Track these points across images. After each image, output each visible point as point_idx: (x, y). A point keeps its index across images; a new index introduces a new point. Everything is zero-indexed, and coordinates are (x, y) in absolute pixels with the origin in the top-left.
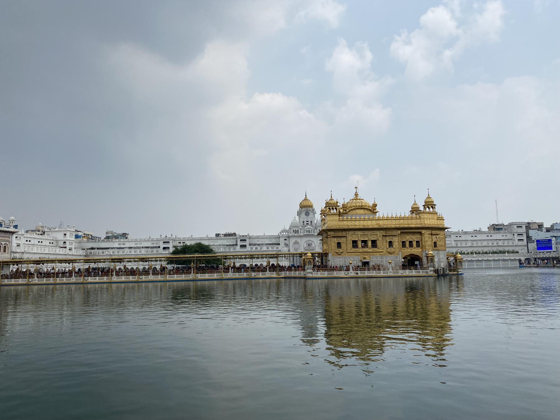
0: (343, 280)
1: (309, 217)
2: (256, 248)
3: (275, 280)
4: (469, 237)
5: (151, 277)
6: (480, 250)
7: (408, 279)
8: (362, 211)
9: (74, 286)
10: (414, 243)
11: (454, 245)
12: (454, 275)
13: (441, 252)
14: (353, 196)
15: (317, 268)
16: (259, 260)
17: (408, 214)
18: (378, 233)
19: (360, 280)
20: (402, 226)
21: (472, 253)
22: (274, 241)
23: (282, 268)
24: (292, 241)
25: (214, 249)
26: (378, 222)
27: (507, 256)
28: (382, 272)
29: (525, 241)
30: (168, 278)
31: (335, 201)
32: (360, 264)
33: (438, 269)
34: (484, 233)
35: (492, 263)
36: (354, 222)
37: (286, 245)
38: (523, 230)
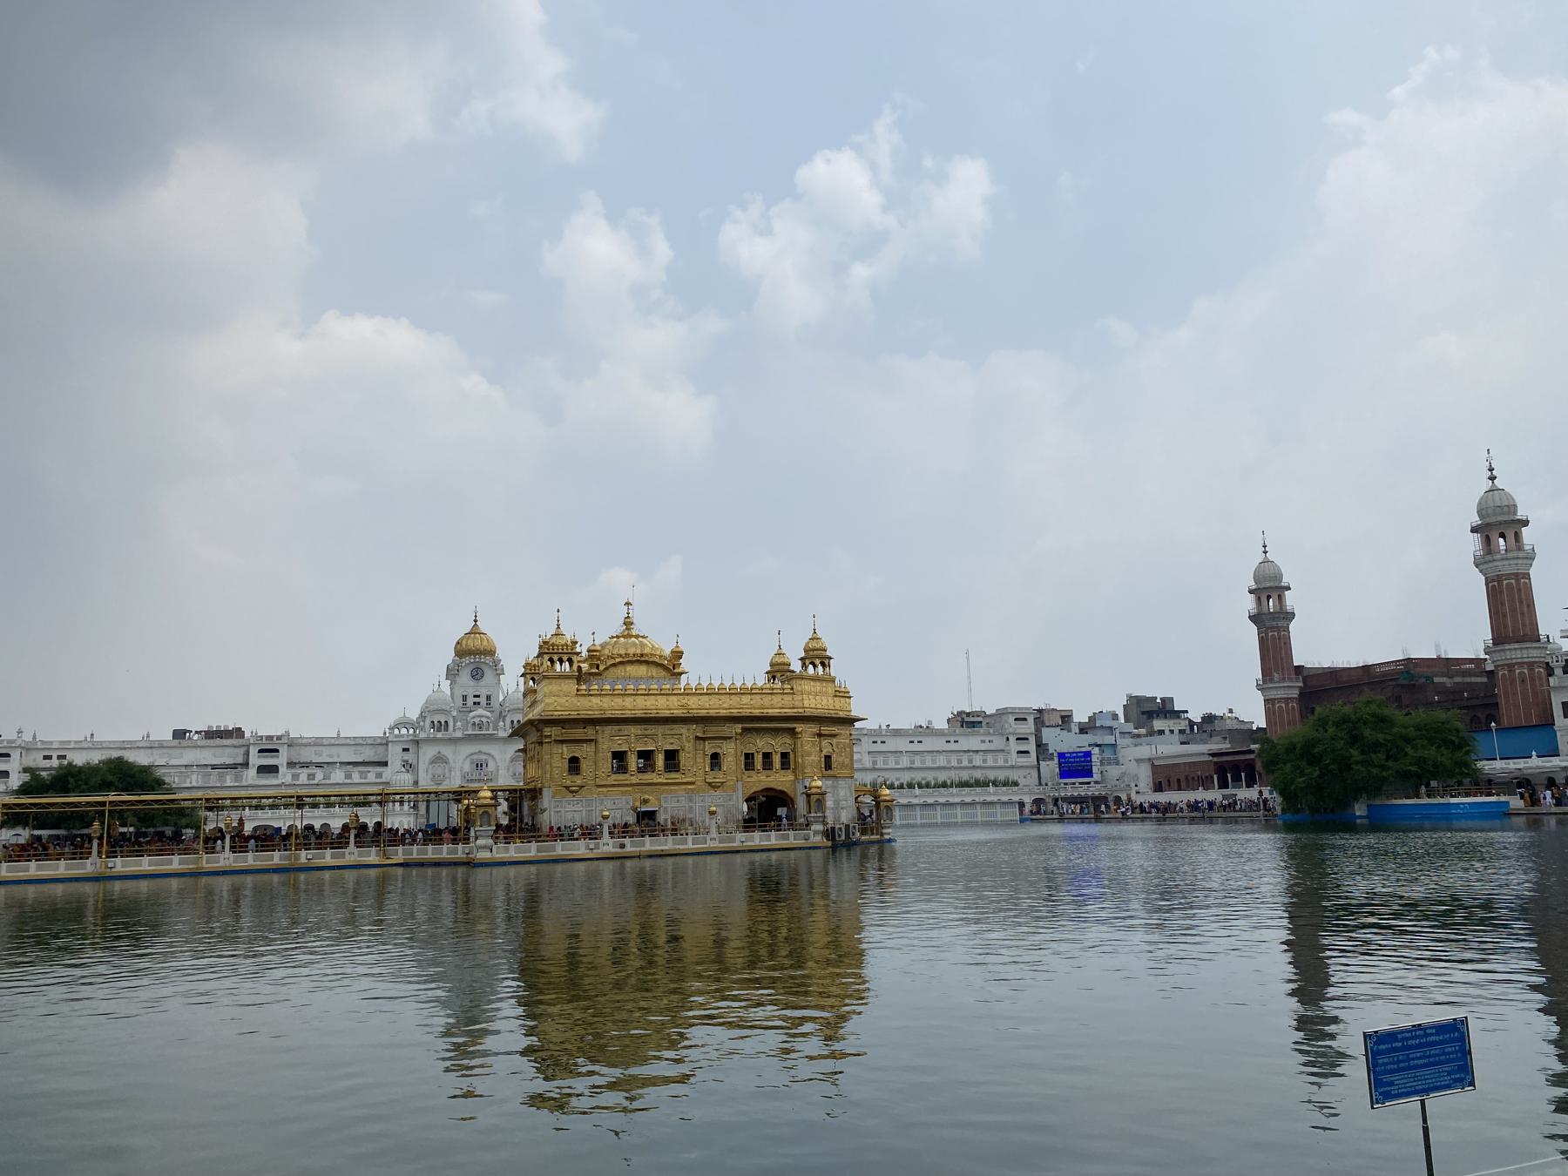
0: (581, 866)
1: (482, 683)
2: (311, 776)
3: (373, 872)
4: (902, 744)
6: (930, 776)
7: (757, 857)
8: (642, 670)
10: (777, 759)
11: (868, 765)
12: (872, 842)
13: (841, 783)
14: (618, 628)
15: (507, 833)
17: (761, 681)
18: (683, 729)
19: (628, 863)
20: (746, 712)
21: (910, 786)
22: (368, 754)
24: (428, 752)
25: (167, 780)
26: (685, 700)
27: (991, 794)
28: (690, 838)
29: (1033, 754)
31: (568, 638)
32: (631, 819)
33: (833, 829)
34: (939, 733)
35: (959, 811)
36: (619, 700)
37: (408, 766)
38: (1028, 728)
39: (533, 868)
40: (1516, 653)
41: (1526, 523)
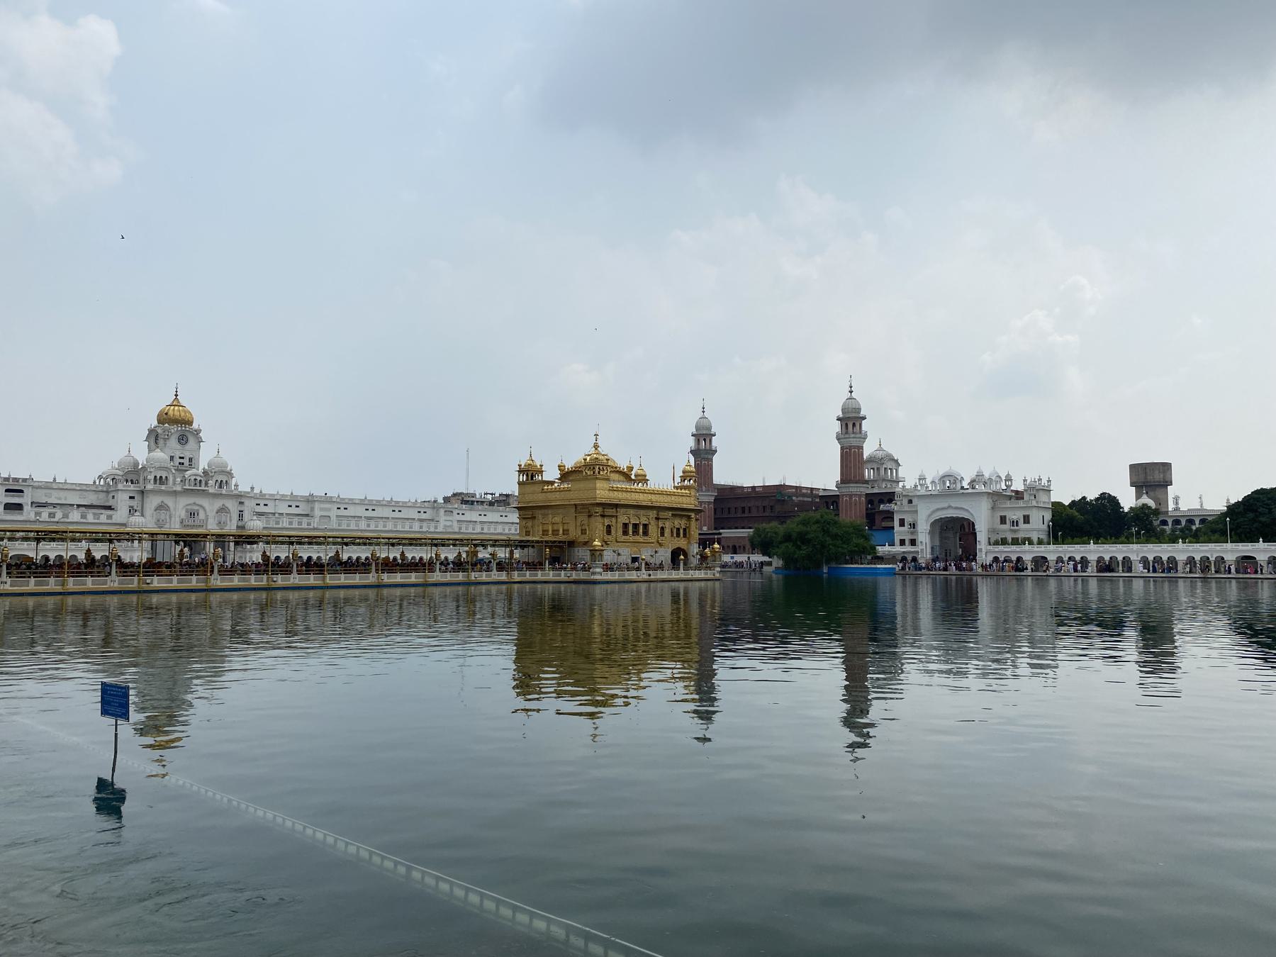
0: (635, 585)
1: (187, 447)
2: (52, 515)
5: (295, 579)
7: (703, 584)
16: (71, 545)
23: (126, 568)
24: (152, 502)
26: (650, 497)
30: (194, 583)
39: (617, 586)
40: (854, 489)
41: (864, 418)
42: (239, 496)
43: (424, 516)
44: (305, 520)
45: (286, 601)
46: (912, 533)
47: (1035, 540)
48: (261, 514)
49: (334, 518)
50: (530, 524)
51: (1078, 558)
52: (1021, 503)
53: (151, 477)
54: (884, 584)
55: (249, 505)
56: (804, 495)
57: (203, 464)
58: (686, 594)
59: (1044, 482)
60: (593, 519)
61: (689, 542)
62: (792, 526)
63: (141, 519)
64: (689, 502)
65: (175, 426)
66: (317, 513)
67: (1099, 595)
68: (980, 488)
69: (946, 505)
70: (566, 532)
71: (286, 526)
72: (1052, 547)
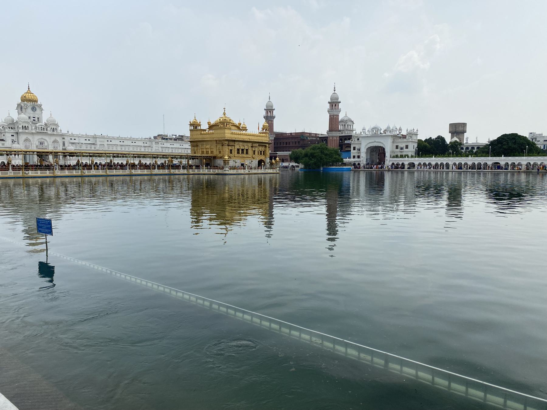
0: (243, 176)
1: (36, 112)
5: (93, 172)
7: (272, 175)
9: (13, 180)
11: (161, 151)
14: (223, 116)
24: (22, 138)
26: (249, 137)
39: (235, 176)
41: (340, 102)
42: (62, 135)
43: (146, 145)
44: (93, 146)
45: (90, 182)
46: (358, 153)
47: (410, 156)
48: (73, 143)
49: (106, 145)
50: (196, 148)
51: (427, 163)
52: (405, 140)
53: (21, 126)
54: (346, 175)
55: (67, 140)
56: (312, 137)
57: (44, 120)
58: (265, 178)
59: (415, 131)
60: (224, 147)
61: (266, 157)
62: (308, 150)
63: (18, 145)
64: (266, 139)
65: (29, 102)
66: (98, 143)
67: (435, 178)
68: (388, 133)
69: (373, 141)
70: (212, 152)
71: (84, 148)
72: (417, 159)
